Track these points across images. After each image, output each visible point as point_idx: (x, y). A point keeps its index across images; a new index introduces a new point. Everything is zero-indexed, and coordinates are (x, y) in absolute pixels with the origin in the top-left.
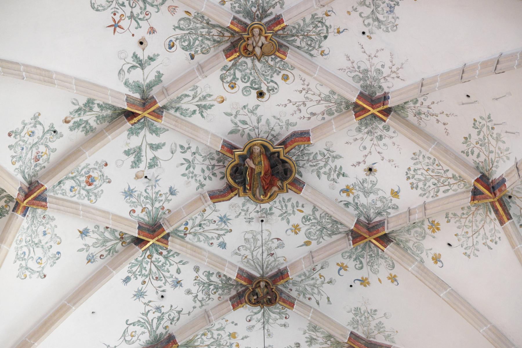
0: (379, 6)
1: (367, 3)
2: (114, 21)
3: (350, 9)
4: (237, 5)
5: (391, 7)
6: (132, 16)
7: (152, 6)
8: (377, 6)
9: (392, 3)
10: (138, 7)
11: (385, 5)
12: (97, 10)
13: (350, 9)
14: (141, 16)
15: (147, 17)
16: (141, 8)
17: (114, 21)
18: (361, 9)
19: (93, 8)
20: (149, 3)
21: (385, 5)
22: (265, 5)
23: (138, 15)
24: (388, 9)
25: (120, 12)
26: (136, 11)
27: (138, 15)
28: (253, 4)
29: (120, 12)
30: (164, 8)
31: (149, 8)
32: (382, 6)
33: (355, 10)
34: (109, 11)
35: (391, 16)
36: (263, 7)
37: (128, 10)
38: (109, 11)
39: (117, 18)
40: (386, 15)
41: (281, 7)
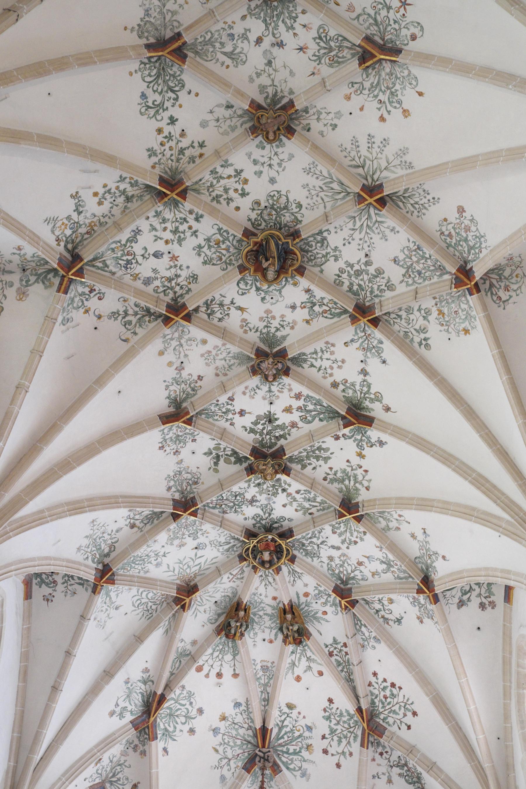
0: (159, 13)
1: (170, 14)
2: (405, 9)
3: (185, 6)
4: (291, 9)
5: (148, 15)
6: (389, 8)
7: (369, 14)
8: (161, 12)
9: (147, 19)
10: (382, 16)
11: (153, 16)
12: (419, 23)
13: (185, 6)
14: (380, 6)
15: (375, 4)
16: (379, 14)
17: (405, 9)
18: (175, 7)
19: (422, 27)
20: (372, 18)
21: (153, 16)
22: (265, 8)
23: (383, 8)
24: (150, 12)
25: (398, 15)
26: (384, 13)
27: (383, 8)
28: (276, 8)
29: (398, 15)
30: (358, 11)
31: (372, 13)
32: (156, 14)
33: (181, 6)
34: (408, 19)
35: (147, 6)
36: (267, 5)
37: (392, 15)
38: (408, 19)
39: (402, 11)
40: (152, 6)
41: (250, 5)
